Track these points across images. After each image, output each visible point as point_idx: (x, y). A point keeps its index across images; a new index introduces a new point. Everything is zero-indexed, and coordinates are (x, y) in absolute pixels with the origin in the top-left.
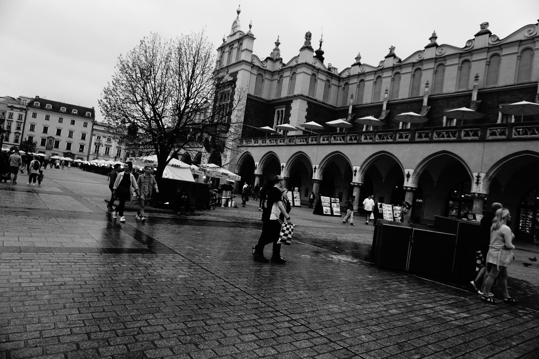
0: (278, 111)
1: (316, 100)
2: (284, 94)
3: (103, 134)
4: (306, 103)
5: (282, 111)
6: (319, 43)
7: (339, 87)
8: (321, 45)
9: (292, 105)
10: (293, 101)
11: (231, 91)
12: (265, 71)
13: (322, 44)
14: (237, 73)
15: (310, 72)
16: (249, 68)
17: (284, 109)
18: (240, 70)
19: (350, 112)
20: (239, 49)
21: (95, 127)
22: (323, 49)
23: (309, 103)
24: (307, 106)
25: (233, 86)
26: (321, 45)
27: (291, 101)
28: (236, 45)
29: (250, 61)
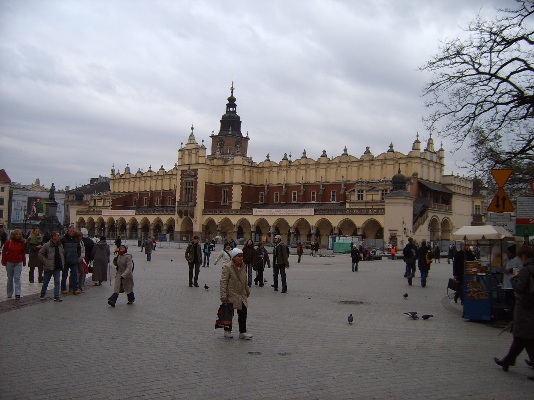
2: (227, 181)
4: (241, 186)
5: (227, 191)
7: (258, 173)
8: (232, 92)
13: (234, 91)
14: (197, 170)
15: (241, 168)
16: (204, 167)
17: (228, 190)
18: (199, 168)
22: (235, 95)
23: (242, 186)
26: (232, 92)
28: (194, 151)
29: (204, 162)
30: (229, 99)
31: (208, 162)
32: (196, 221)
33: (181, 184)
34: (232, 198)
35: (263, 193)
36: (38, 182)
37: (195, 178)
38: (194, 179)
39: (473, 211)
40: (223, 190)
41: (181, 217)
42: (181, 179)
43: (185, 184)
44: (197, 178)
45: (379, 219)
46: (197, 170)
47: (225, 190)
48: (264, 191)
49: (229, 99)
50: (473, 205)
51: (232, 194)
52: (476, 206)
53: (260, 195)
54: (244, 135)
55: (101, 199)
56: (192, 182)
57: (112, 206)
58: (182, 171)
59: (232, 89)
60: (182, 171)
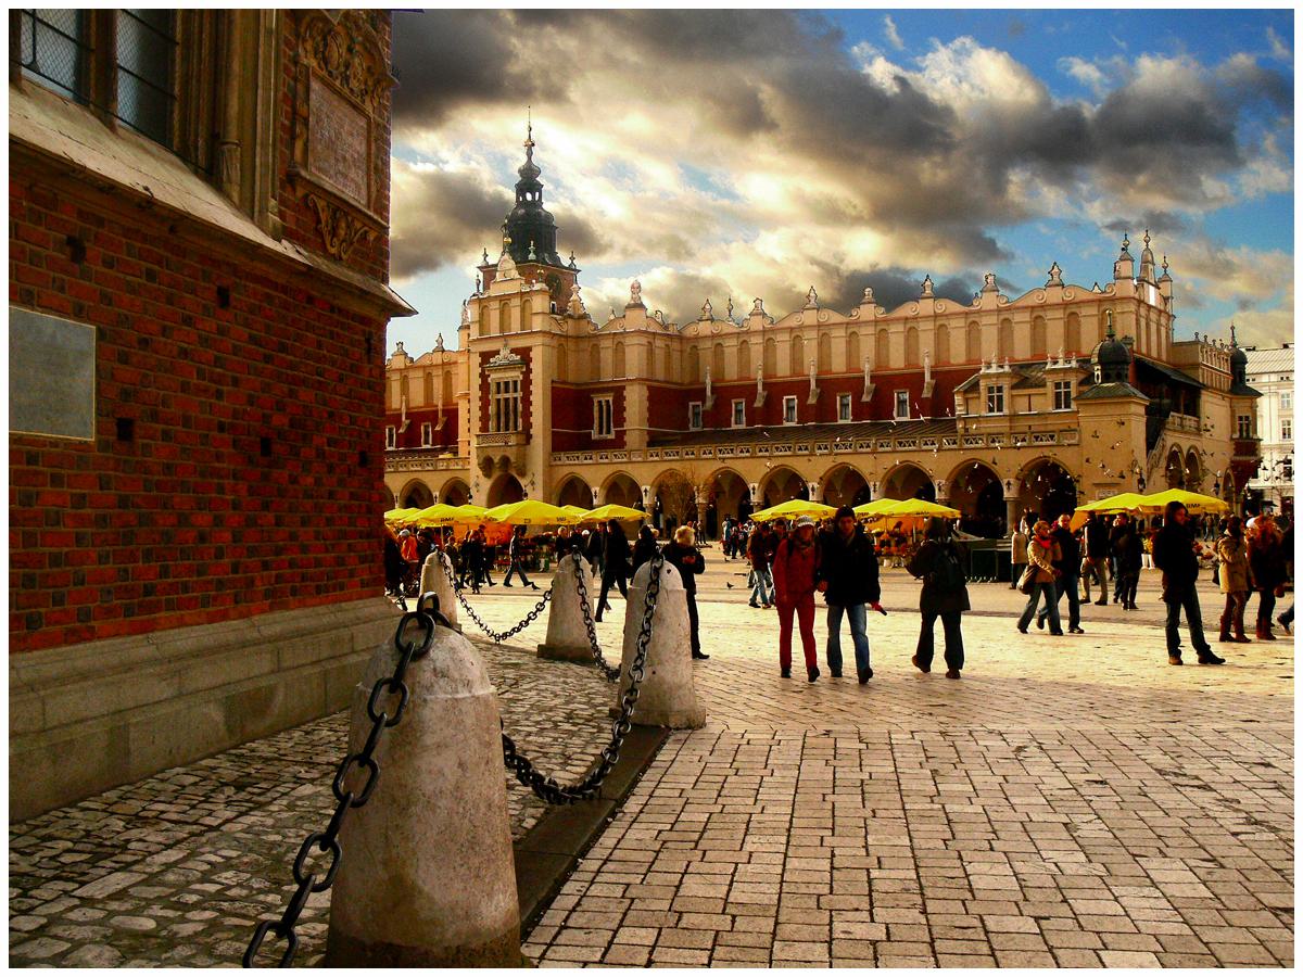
0: (600, 402)
1: (657, 381)
2: (607, 376)
5: (608, 402)
8: (530, 154)
11: (521, 378)
12: (567, 337)
14: (529, 349)
15: (644, 340)
17: (611, 399)
19: (709, 393)
20: (523, 310)
23: (649, 388)
24: (646, 393)
26: (530, 154)
27: (624, 388)
28: (516, 302)
31: (556, 330)
32: (533, 483)
33: (484, 387)
35: (699, 403)
38: (522, 373)
39: (1233, 432)
40: (596, 401)
41: (487, 475)
42: (483, 376)
43: (493, 388)
44: (529, 371)
45: (1068, 459)
47: (603, 400)
48: (704, 403)
50: (1233, 416)
51: (624, 409)
52: (1241, 418)
53: (691, 407)
56: (515, 382)
59: (530, 145)
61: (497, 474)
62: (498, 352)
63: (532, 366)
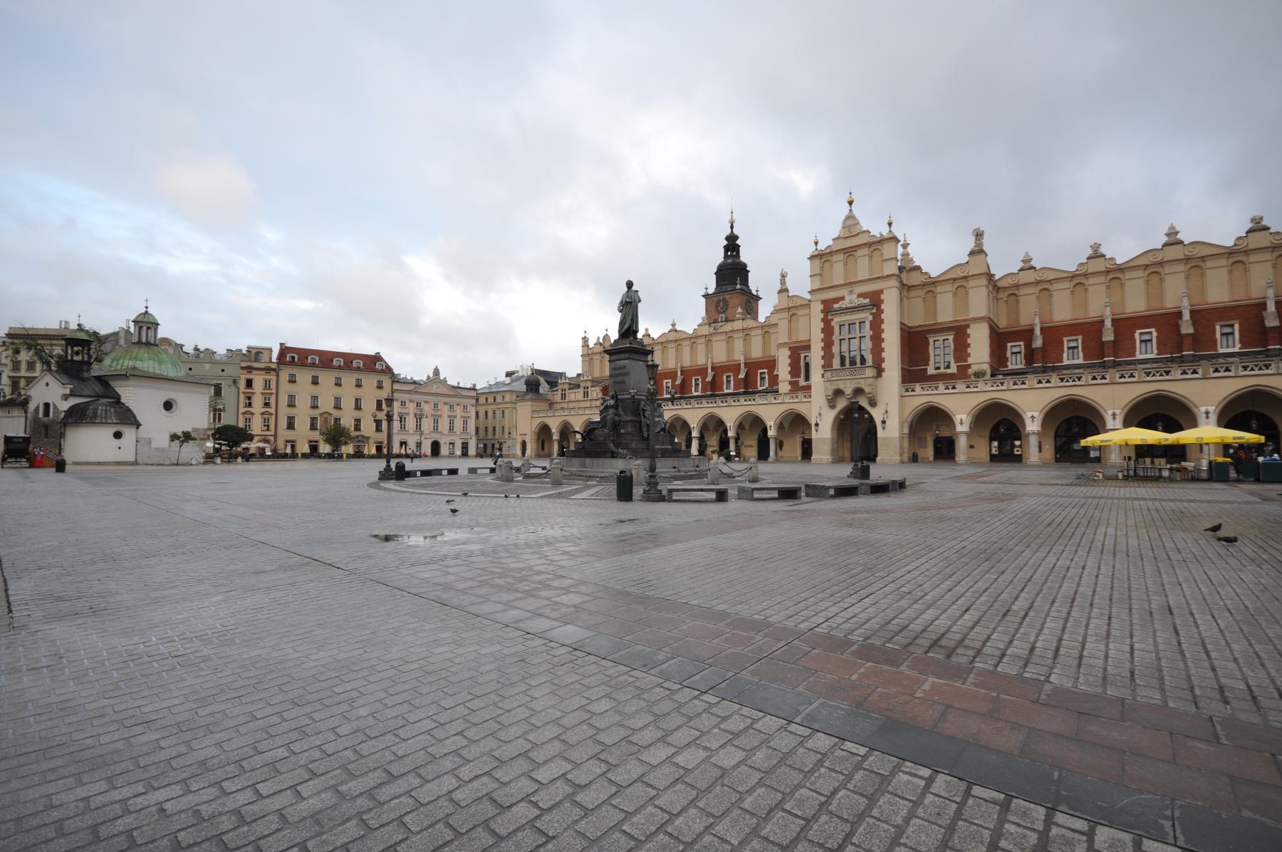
3: (408, 396)
6: (730, 225)
8: (732, 227)
9: (969, 331)
10: (971, 326)
14: (881, 292)
21: (396, 386)
25: (874, 311)
26: (732, 227)
27: (968, 326)
30: (727, 238)
34: (969, 355)
36: (436, 372)
37: (874, 311)
41: (833, 407)
44: (880, 311)
46: (881, 292)
49: (727, 238)
54: (755, 293)
55: (578, 386)
57: (603, 399)
58: (824, 302)
60: (824, 302)
61: (842, 404)
62: (842, 298)
63: (883, 307)
